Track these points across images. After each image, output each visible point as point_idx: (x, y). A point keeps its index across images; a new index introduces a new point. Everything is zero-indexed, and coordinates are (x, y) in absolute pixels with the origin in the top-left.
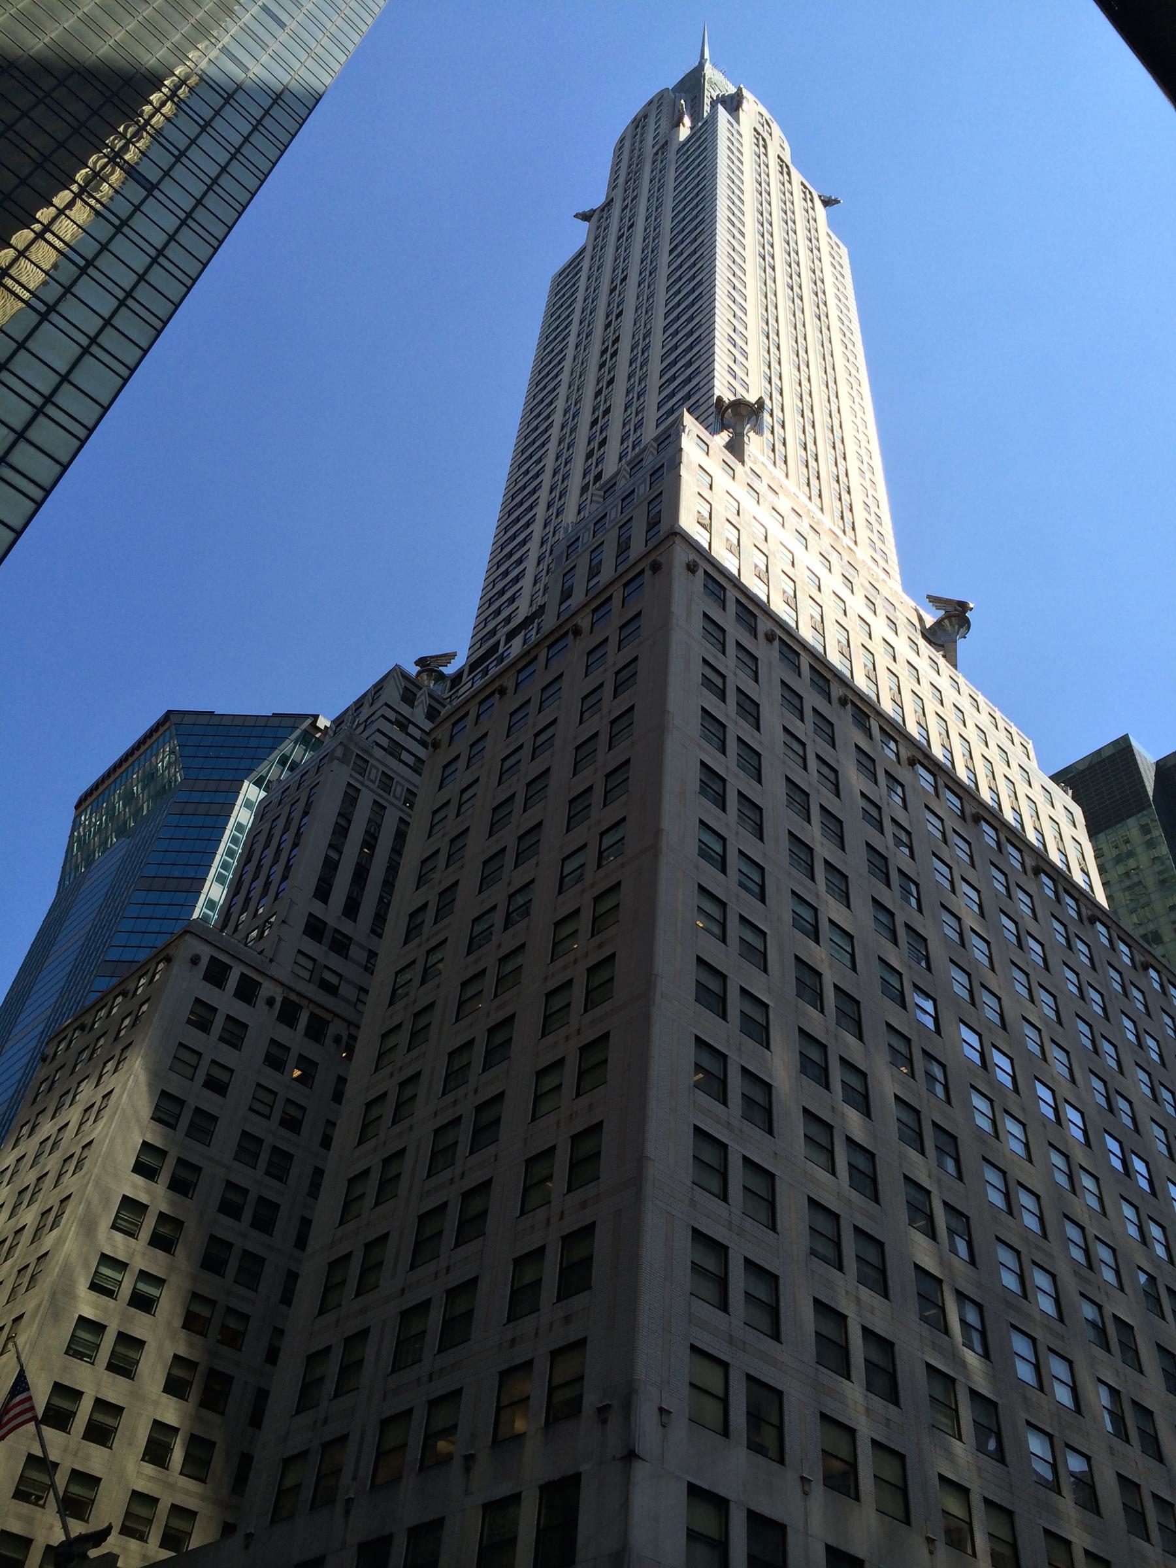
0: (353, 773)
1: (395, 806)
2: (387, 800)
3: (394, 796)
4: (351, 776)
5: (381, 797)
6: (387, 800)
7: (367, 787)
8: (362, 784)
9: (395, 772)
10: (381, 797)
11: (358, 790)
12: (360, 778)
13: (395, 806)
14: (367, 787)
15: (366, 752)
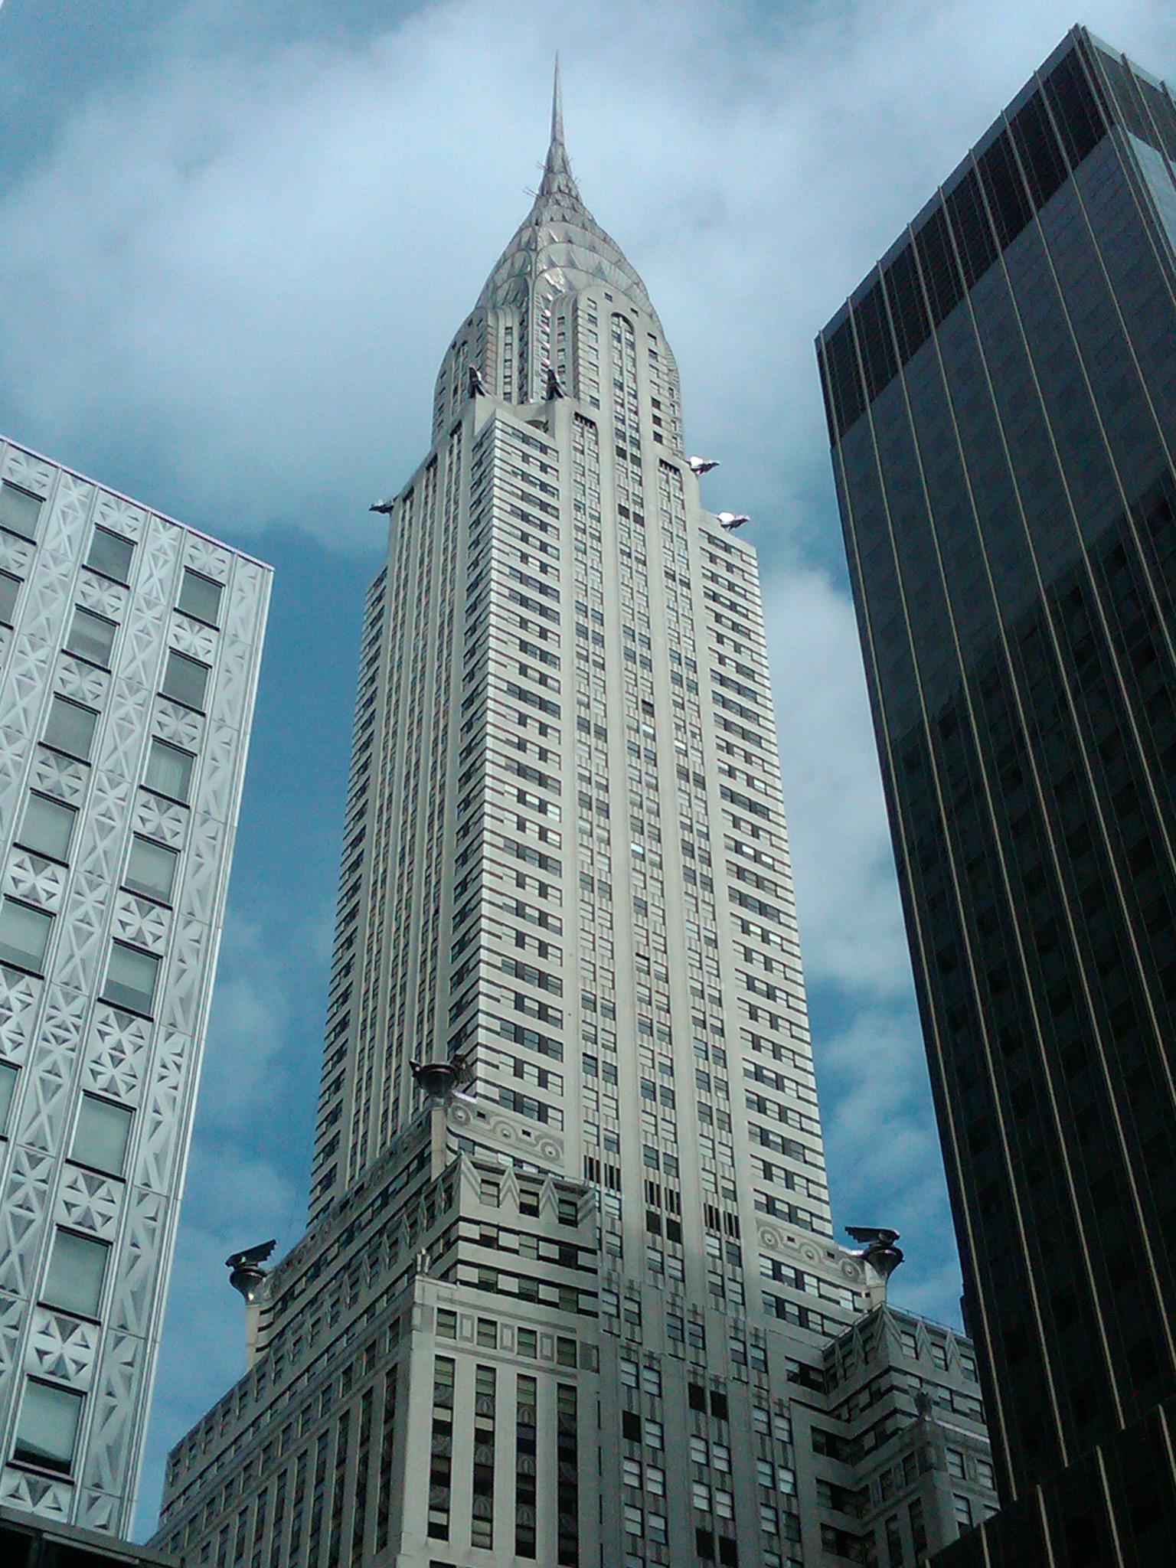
0: (440, 1339)
1: (508, 1361)
2: (494, 1358)
3: (503, 1348)
4: (438, 1345)
5: (484, 1356)
6: (494, 1358)
7: (462, 1351)
8: (455, 1349)
9: (493, 1311)
10: (484, 1356)
11: (453, 1360)
12: (450, 1342)
13: (508, 1361)
14: (462, 1351)
15: (452, 1301)
